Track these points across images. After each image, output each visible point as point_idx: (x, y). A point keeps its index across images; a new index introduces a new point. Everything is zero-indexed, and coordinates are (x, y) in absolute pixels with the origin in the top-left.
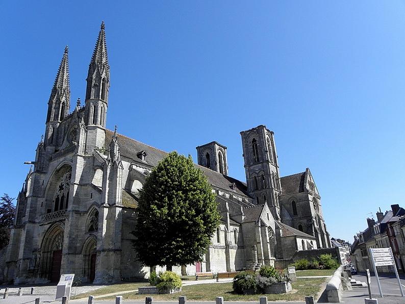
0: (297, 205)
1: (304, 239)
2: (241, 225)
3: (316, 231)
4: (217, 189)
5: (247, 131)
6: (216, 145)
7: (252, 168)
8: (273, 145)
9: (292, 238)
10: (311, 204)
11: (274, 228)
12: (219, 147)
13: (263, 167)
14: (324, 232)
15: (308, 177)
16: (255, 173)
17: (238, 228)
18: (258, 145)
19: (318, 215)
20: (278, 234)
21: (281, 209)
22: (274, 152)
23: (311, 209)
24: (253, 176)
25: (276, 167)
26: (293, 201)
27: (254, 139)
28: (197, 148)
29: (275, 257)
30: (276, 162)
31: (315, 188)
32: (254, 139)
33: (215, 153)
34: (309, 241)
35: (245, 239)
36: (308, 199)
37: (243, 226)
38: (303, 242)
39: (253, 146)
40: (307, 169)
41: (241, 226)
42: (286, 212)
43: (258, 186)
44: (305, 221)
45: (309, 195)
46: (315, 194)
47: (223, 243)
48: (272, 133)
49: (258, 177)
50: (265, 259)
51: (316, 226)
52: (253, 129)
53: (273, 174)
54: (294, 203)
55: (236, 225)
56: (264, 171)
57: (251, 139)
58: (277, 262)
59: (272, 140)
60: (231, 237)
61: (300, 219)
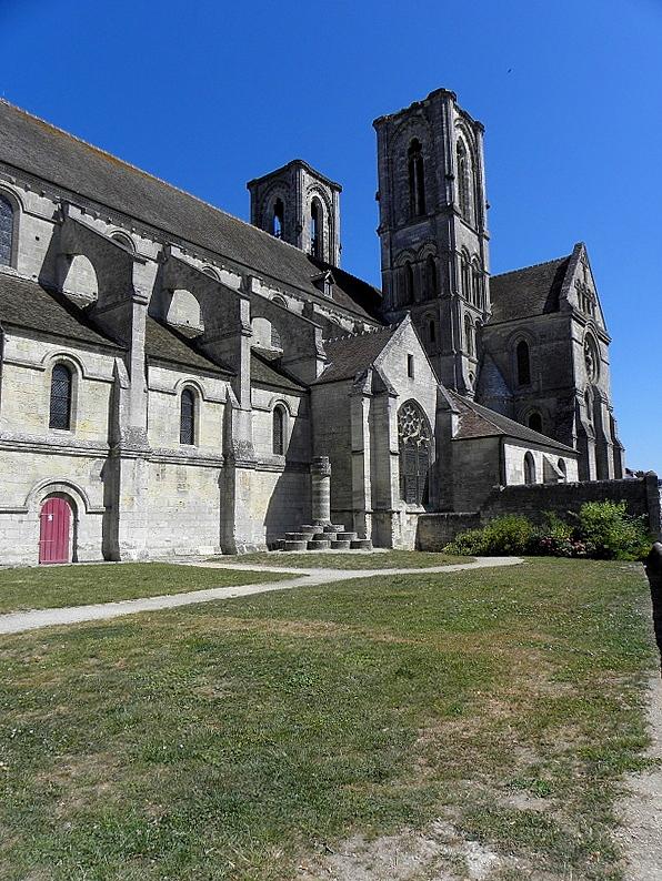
0: (533, 351)
1: (532, 451)
2: (309, 392)
3: (581, 432)
4: (249, 272)
5: (396, 117)
6: (303, 172)
7: (400, 235)
8: (476, 167)
9: (491, 444)
10: (578, 352)
11: (430, 409)
12: (313, 180)
13: (434, 227)
14: (608, 439)
15: (579, 266)
16: (411, 251)
17: (294, 402)
18: (426, 158)
19: (594, 388)
20: (442, 428)
21: (481, 365)
22: (478, 191)
23: (577, 368)
24: (403, 263)
25: (481, 236)
26: (523, 342)
27: (415, 142)
28: (250, 185)
29: (425, 503)
30: (480, 221)
31: (594, 305)
32: (415, 142)
33: (297, 198)
34: (554, 459)
35: (317, 438)
36: (570, 333)
37: (320, 395)
38: (529, 459)
39: (411, 166)
40: (578, 247)
41: (307, 395)
42: (494, 375)
43: (416, 289)
44: (550, 403)
45: (573, 322)
46: (593, 325)
47: (209, 440)
48: (478, 127)
49: (416, 262)
50: (376, 512)
51: (584, 418)
52: (415, 106)
53: (465, 254)
54: (523, 347)
55: (287, 390)
56: (434, 243)
57: (405, 143)
58: (429, 522)
59: (474, 150)
60: (257, 431)
61: (537, 394)
